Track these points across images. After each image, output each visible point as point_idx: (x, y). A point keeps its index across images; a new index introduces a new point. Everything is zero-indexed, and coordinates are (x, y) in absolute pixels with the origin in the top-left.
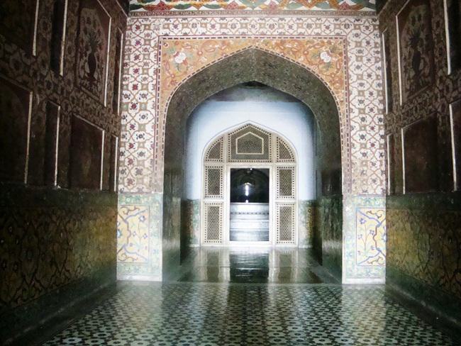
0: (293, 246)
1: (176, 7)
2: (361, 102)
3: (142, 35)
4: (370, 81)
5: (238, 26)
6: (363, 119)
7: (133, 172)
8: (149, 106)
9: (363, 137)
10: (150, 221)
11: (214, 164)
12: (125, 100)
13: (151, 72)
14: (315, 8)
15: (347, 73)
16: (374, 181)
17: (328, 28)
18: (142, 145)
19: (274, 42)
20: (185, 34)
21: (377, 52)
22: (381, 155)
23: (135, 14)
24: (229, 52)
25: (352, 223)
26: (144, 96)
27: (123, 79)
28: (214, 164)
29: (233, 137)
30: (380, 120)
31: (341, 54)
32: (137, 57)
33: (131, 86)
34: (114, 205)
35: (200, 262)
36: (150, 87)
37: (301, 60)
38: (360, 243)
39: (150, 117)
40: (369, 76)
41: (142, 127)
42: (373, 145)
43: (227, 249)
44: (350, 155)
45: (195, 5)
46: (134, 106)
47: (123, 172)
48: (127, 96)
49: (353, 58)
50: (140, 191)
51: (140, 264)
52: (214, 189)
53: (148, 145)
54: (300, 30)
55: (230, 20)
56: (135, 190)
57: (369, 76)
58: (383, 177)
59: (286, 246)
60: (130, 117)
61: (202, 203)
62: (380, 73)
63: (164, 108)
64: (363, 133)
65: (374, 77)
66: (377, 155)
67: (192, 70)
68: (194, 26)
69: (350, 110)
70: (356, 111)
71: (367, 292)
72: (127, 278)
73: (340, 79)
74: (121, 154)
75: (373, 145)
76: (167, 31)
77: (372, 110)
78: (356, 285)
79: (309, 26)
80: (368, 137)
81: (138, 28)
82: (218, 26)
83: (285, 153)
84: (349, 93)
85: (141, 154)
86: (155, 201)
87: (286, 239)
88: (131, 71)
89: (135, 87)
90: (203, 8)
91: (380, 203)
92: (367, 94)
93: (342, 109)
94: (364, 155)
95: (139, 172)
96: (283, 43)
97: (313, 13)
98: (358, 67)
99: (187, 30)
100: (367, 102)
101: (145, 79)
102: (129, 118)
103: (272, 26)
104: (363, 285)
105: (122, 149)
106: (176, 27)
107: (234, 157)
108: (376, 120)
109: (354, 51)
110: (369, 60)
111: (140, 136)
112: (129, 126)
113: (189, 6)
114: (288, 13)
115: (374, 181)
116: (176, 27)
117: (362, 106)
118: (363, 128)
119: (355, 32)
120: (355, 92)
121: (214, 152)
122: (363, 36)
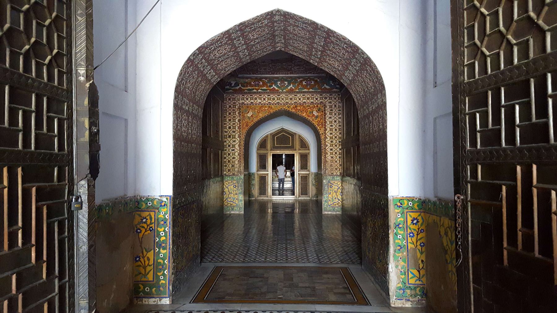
0: (308, 198)
1: (247, 90)
2: (331, 134)
3: (232, 103)
4: (335, 124)
5: (276, 99)
6: (332, 142)
7: (230, 166)
8: (237, 137)
9: (331, 150)
10: (238, 187)
11: (262, 152)
12: (225, 134)
13: (237, 120)
14: (311, 90)
15: (325, 120)
16: (336, 169)
17: (317, 99)
18: (234, 154)
19: (292, 107)
20: (252, 103)
21: (339, 110)
22: (340, 157)
23: (228, 93)
24: (272, 111)
25: (326, 187)
26: (234, 132)
27: (225, 124)
28: (262, 152)
29: (273, 135)
30: (340, 142)
31: (322, 112)
32: (230, 114)
33: (228, 127)
34: (222, 181)
35: (256, 207)
36: (237, 128)
37: (304, 115)
38: (330, 196)
39: (237, 141)
40: (335, 121)
41: (234, 146)
42: (336, 153)
43: (271, 201)
44: (325, 157)
45: (256, 89)
46: (230, 137)
47: (226, 166)
48: (226, 132)
49: (328, 113)
50: (234, 174)
51: (234, 206)
52: (262, 165)
53: (236, 154)
54: (304, 101)
55: (272, 96)
56: (231, 174)
57: (335, 121)
58: (340, 168)
59: (303, 198)
60: (228, 141)
61: (256, 176)
62: (340, 120)
63: (243, 137)
64: (332, 148)
65: (337, 122)
66: (338, 157)
67: (255, 120)
68: (256, 99)
69: (326, 138)
70: (329, 138)
71: (334, 218)
72: (228, 212)
73: (322, 123)
74: (225, 158)
75: (336, 153)
76: (243, 101)
77: (336, 137)
78: (328, 214)
79: (308, 99)
80: (334, 149)
81: (229, 99)
82: (266, 99)
83: (304, 145)
84: (326, 130)
85: (234, 158)
86: (240, 179)
87: (305, 194)
88: (227, 121)
89: (230, 128)
90: (260, 91)
91: (339, 178)
92: (334, 130)
93: (323, 137)
94: (332, 157)
95: (233, 166)
96: (296, 106)
97: (310, 92)
98: (330, 118)
99: (253, 101)
100: (334, 134)
101: (234, 124)
102: (228, 142)
103: (291, 99)
104: (331, 215)
105: (225, 156)
106: (247, 99)
107: (274, 148)
108: (338, 142)
109: (329, 110)
110: (335, 114)
111: (233, 150)
112: (227, 146)
113: (253, 89)
114: (297, 92)
115: (336, 169)
116: (247, 99)
117: (331, 136)
118: (331, 145)
119: (329, 101)
120: (328, 129)
121: (263, 145)
122: (333, 103)
